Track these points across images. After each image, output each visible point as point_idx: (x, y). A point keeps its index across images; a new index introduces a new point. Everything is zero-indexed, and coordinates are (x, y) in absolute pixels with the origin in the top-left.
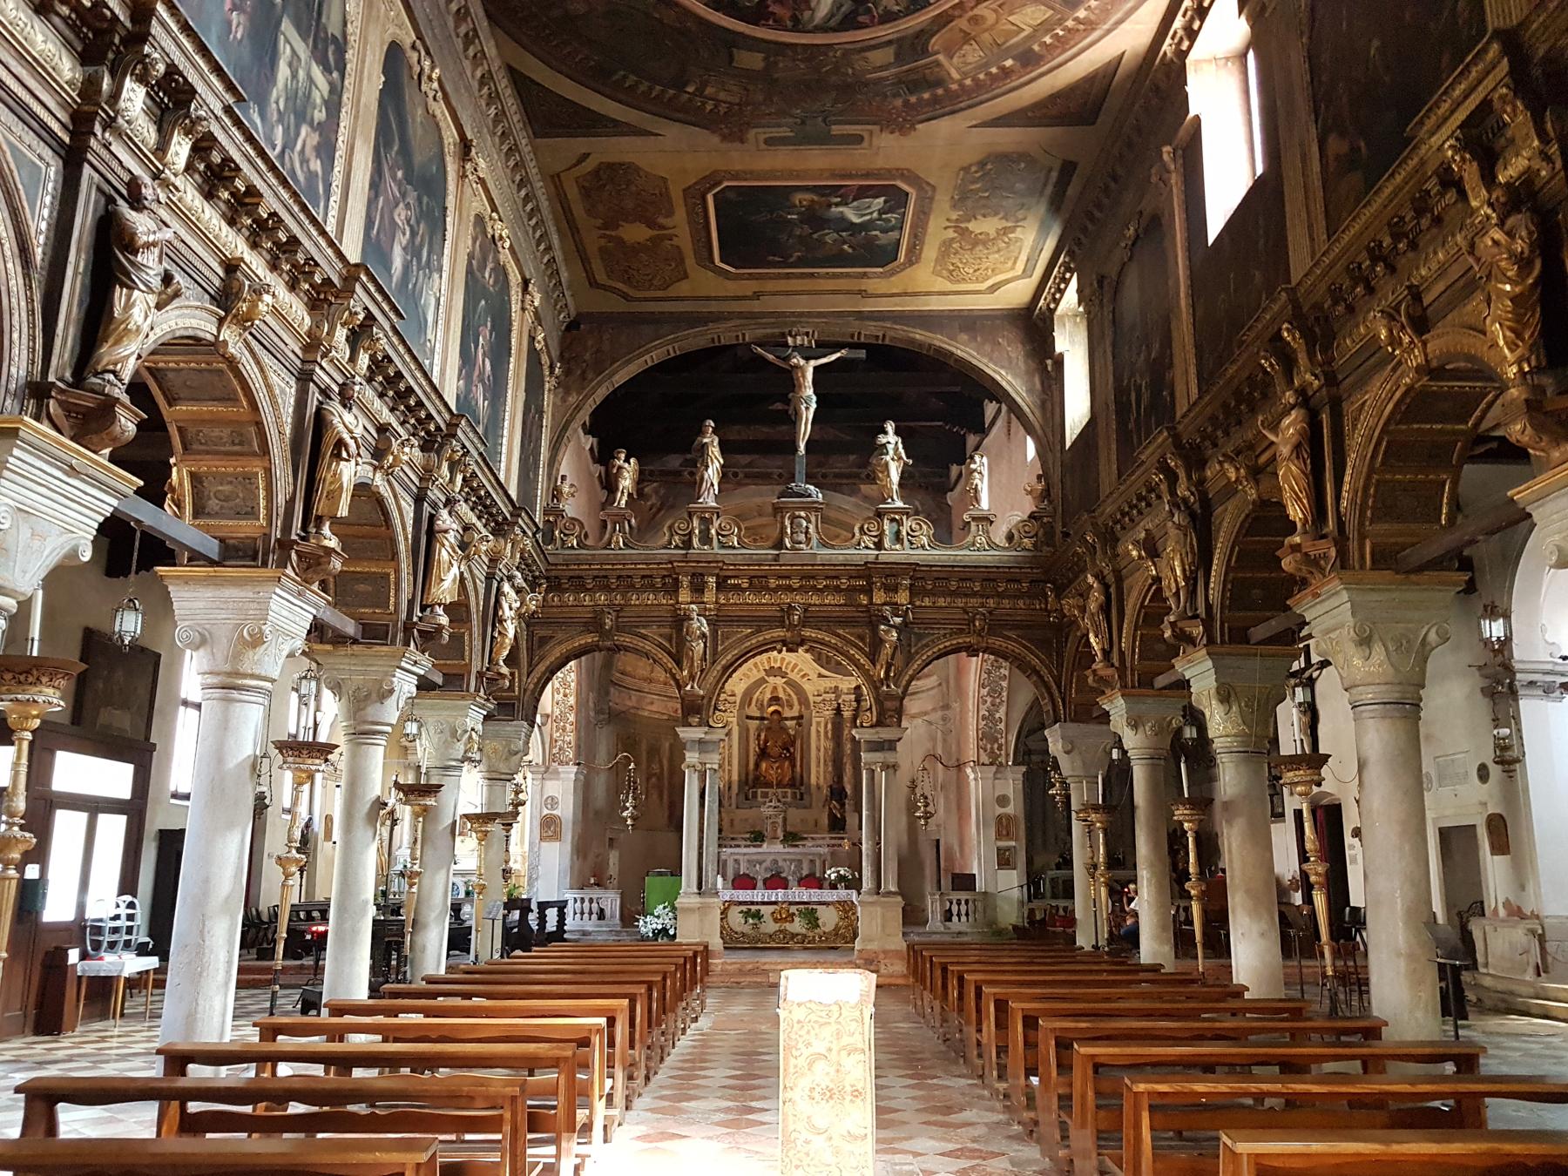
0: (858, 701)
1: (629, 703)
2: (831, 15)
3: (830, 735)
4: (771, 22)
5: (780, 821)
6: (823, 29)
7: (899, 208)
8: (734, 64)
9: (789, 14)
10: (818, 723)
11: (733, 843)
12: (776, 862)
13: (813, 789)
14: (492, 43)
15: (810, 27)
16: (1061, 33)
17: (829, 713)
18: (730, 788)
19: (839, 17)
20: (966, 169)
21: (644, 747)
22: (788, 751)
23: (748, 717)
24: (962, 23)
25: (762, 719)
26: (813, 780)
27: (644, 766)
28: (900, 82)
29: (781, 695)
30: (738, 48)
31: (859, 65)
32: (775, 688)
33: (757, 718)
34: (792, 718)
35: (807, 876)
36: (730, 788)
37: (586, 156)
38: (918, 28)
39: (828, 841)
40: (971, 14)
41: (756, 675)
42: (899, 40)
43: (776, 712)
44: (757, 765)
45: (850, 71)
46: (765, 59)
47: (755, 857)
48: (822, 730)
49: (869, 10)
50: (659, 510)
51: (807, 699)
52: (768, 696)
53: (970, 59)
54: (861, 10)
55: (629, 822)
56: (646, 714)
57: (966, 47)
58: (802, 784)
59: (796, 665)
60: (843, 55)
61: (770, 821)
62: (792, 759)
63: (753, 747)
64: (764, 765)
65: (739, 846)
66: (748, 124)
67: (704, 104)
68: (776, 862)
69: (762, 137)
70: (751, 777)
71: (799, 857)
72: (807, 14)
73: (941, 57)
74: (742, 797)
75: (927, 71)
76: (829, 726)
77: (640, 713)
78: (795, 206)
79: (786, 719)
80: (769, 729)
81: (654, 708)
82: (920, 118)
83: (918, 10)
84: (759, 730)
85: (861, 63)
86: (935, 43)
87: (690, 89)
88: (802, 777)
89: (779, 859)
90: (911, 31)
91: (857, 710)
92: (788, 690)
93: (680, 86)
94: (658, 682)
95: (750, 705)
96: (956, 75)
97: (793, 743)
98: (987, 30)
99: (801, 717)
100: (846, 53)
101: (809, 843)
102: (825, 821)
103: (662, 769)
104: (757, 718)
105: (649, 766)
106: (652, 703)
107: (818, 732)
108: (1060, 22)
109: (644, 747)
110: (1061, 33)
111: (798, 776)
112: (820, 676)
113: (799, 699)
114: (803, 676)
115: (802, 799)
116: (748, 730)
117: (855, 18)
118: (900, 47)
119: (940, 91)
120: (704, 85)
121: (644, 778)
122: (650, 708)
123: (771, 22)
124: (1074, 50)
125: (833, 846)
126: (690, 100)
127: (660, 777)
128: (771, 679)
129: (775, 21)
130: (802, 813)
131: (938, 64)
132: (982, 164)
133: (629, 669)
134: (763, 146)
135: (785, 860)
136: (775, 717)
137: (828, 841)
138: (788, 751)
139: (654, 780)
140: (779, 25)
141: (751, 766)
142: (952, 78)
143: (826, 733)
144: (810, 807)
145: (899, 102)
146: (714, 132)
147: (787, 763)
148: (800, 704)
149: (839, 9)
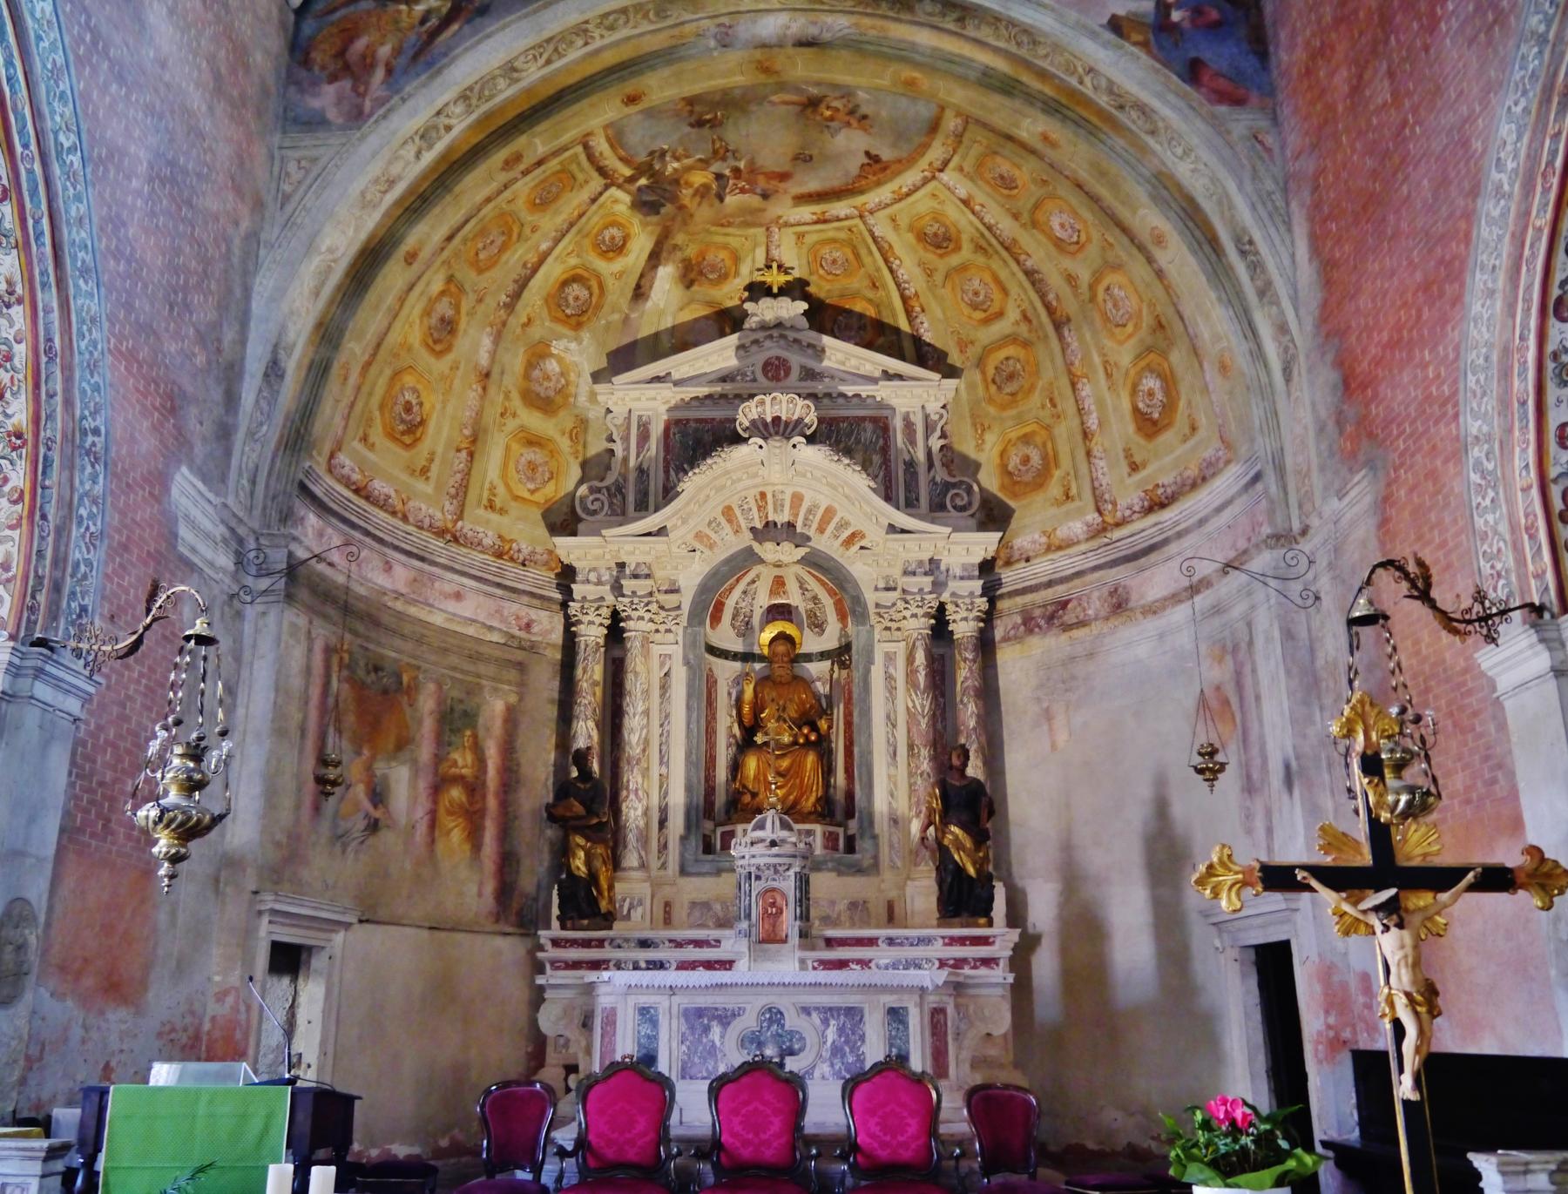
0: (991, 592)
1: (381, 580)
3: (921, 678)
5: (788, 885)
10: (890, 658)
11: (643, 955)
12: (774, 1016)
13: (881, 826)
17: (918, 626)
18: (662, 823)
21: (427, 703)
22: (814, 728)
23: (712, 650)
25: (747, 657)
26: (880, 804)
27: (425, 752)
29: (794, 598)
32: (779, 583)
33: (735, 656)
34: (823, 655)
35: (879, 1068)
36: (662, 823)
39: (938, 950)
41: (732, 542)
43: (782, 637)
44: (736, 767)
47: (703, 1001)
48: (900, 673)
50: (446, 22)
51: (858, 600)
52: (763, 600)
55: (163, 843)
56: (438, 619)
58: (850, 812)
59: (829, 513)
61: (757, 887)
62: (822, 747)
63: (726, 725)
64: (752, 764)
65: (659, 965)
68: (774, 1016)
70: (720, 799)
71: (852, 1000)
74: (695, 843)
76: (920, 658)
77: (412, 611)
79: (808, 657)
80: (764, 681)
81: (466, 609)
84: (739, 680)
88: (850, 795)
89: (784, 1003)
91: (989, 618)
92: (813, 585)
94: (477, 545)
95: (716, 618)
97: (826, 712)
99: (846, 648)
101: (882, 955)
102: (922, 892)
103: (481, 761)
104: (735, 656)
105: (438, 759)
106: (458, 596)
107: (889, 678)
109: (427, 703)
111: (839, 796)
112: (892, 529)
113: (839, 606)
114: (849, 542)
115: (850, 847)
116: (711, 683)
121: (423, 785)
122: (452, 606)
125: (959, 963)
127: (474, 788)
128: (768, 551)
130: (855, 886)
133: (380, 487)
135: (806, 1011)
136: (781, 648)
137: (938, 950)
138: (814, 728)
139: (456, 793)
141: (722, 773)
143: (911, 673)
144: (875, 868)
147: (811, 759)
148: (842, 617)
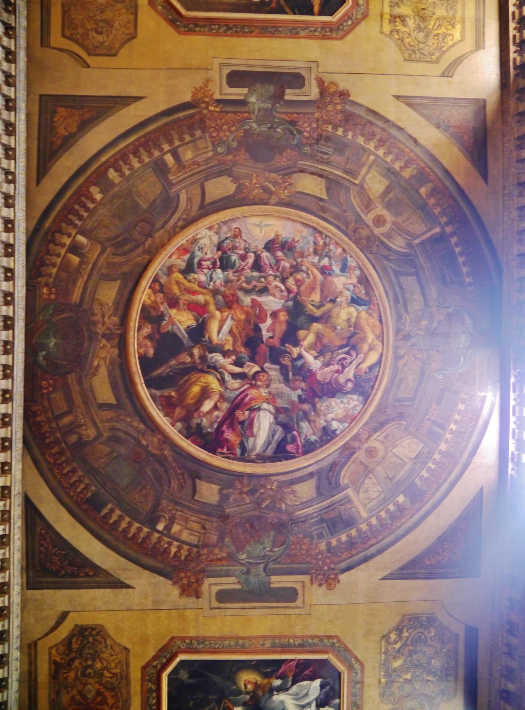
2: (268, 443)
4: (225, 450)
6: (262, 459)
7: (334, 698)
8: (196, 498)
9: (238, 442)
14: (20, 467)
15: (253, 455)
16: (433, 466)
19: (273, 446)
20: (386, 637)
24: (360, 455)
28: (322, 521)
30: (200, 479)
31: (290, 500)
37: (64, 616)
38: (330, 460)
40: (366, 445)
42: (319, 472)
45: (283, 506)
46: (220, 491)
49: (294, 437)
53: (373, 494)
54: (289, 437)
57: (367, 481)
60: (278, 487)
66: (203, 571)
67: (170, 544)
69: (215, 589)
72: (251, 440)
73: (350, 492)
75: (342, 508)
78: (239, 692)
82: (343, 565)
83: (329, 441)
85: (291, 496)
86: (345, 477)
87: (160, 527)
90: (325, 464)
93: (152, 522)
96: (364, 514)
98: (379, 464)
100: (282, 485)
108: (430, 455)
110: (433, 466)
117: (285, 446)
118: (319, 479)
119: (354, 532)
120: (172, 521)
123: (225, 450)
124: (446, 486)
126: (159, 540)
129: (228, 449)
131: (350, 501)
132: (399, 630)
134: (215, 604)
140: (231, 456)
142: (360, 516)
145: (323, 546)
146: (175, 583)
149: (273, 436)
